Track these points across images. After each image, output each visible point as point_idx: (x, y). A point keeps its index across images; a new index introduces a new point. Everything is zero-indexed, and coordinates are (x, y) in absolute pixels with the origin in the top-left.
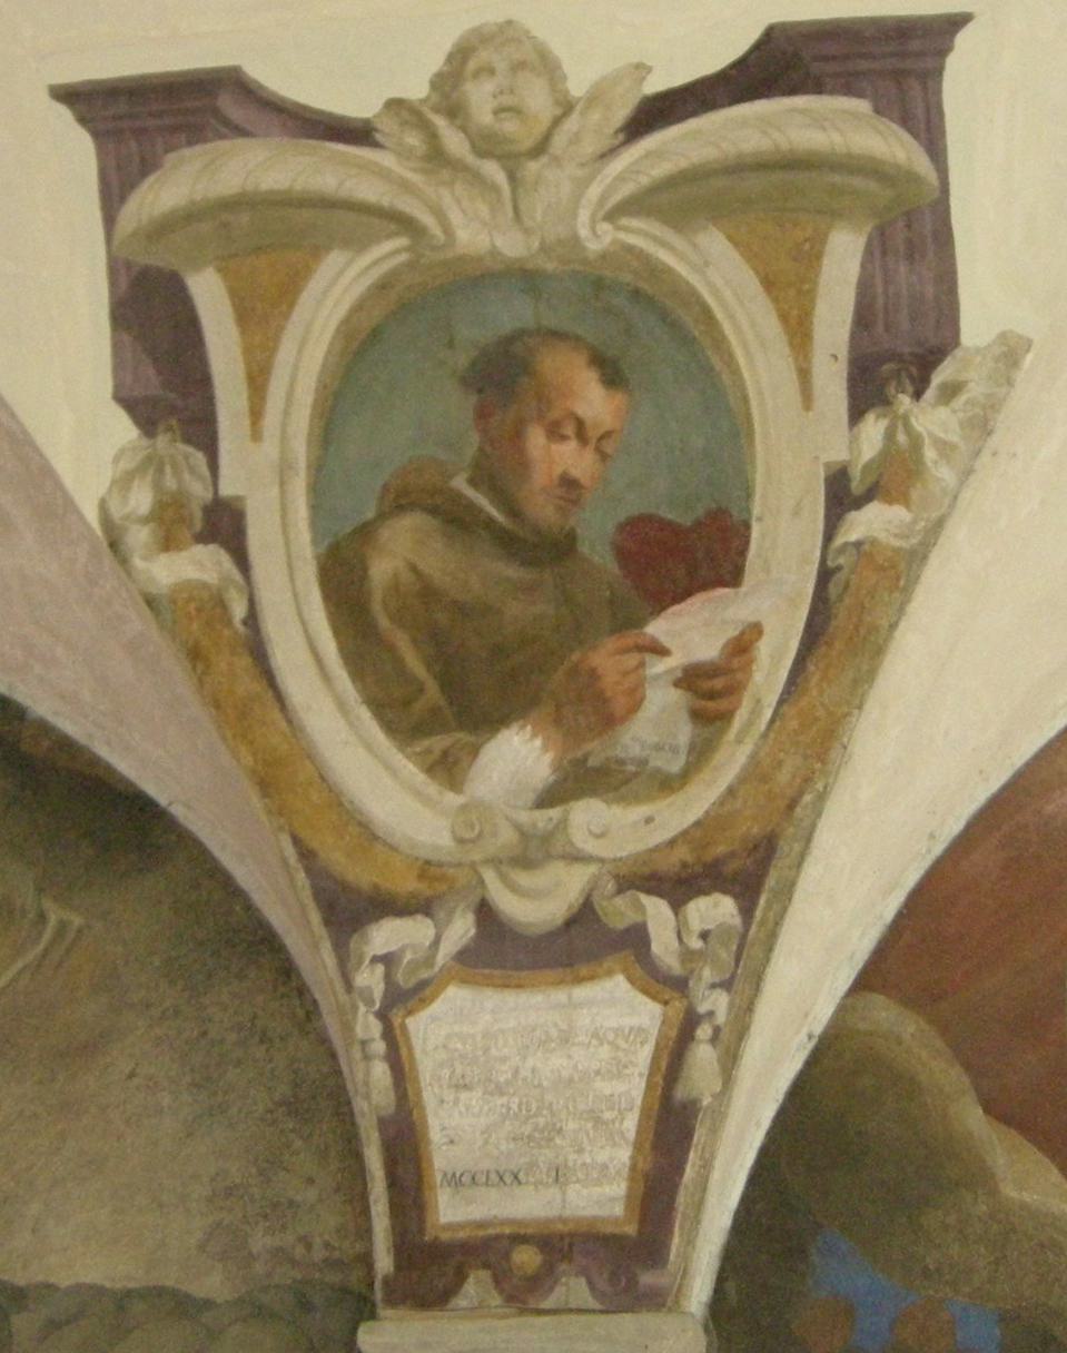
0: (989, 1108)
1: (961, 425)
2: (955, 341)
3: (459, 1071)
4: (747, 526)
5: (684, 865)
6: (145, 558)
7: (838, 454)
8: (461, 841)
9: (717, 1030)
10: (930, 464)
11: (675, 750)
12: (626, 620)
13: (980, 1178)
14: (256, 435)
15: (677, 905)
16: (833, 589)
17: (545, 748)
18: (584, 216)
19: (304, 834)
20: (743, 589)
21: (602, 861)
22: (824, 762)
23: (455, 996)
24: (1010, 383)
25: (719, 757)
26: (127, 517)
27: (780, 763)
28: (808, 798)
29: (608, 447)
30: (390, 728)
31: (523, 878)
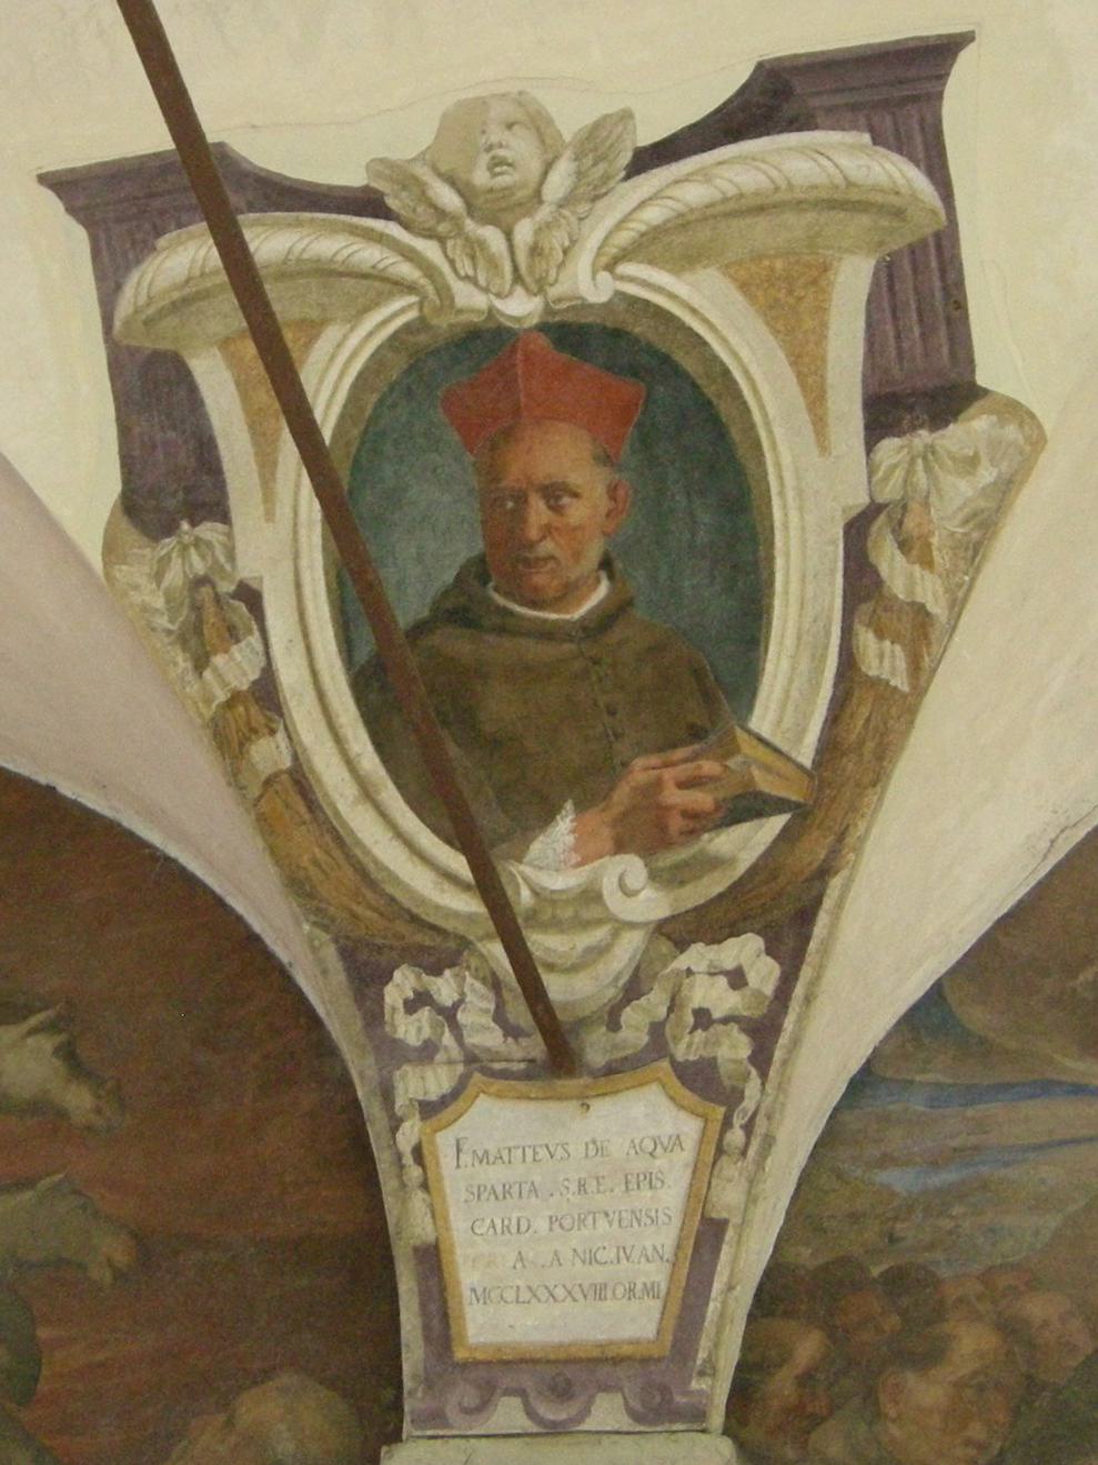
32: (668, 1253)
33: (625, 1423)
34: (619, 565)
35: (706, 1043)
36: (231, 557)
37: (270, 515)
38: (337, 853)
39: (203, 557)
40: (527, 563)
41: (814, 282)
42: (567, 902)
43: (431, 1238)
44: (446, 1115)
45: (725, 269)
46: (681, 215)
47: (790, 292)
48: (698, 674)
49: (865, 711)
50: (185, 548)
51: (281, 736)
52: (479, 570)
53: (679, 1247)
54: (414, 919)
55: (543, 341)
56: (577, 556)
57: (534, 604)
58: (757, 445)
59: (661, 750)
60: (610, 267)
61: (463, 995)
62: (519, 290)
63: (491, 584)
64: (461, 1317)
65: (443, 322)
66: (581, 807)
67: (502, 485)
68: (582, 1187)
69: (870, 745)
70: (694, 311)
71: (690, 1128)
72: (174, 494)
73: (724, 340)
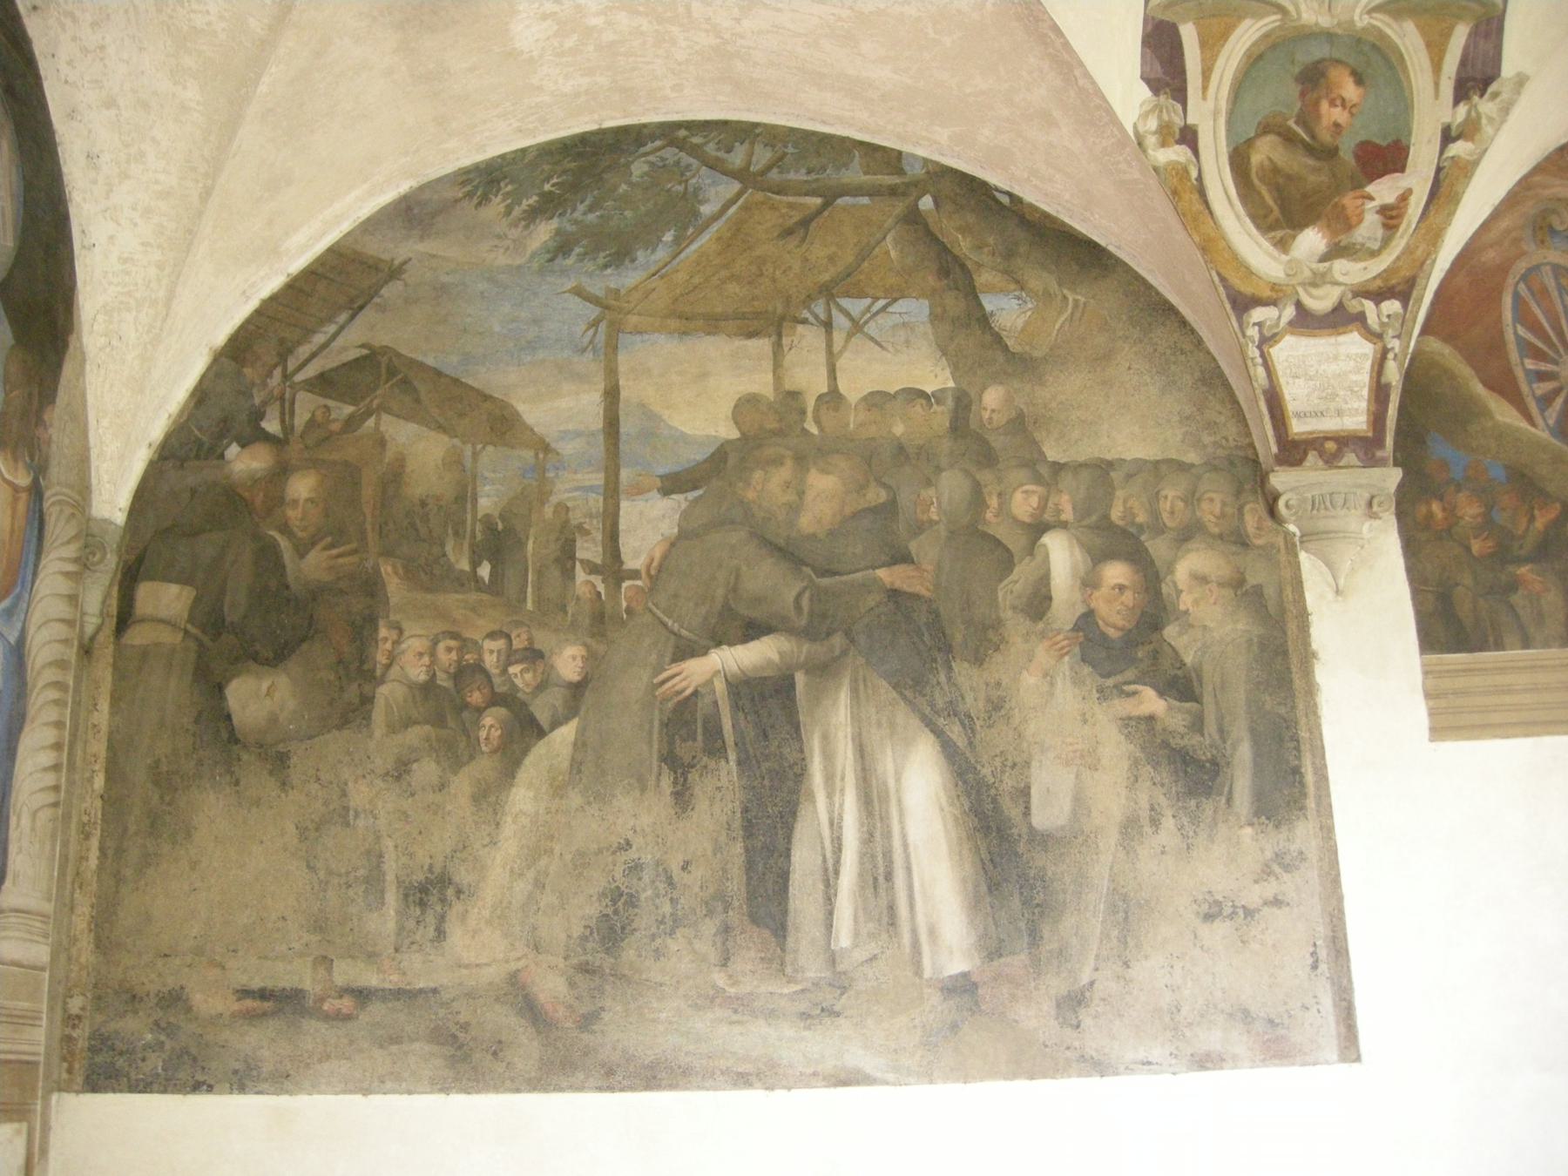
2: (1499, 75)
3: (1294, 370)
4: (1409, 148)
5: (1380, 288)
6: (1154, 150)
7: (1447, 120)
8: (1288, 275)
9: (1396, 355)
11: (1376, 240)
13: (1486, 413)
14: (1204, 98)
15: (1377, 304)
16: (1442, 176)
17: (1323, 237)
18: (1358, 11)
19: (1221, 271)
20: (1406, 174)
21: (1346, 285)
23: (1289, 340)
24: (1519, 93)
25: (1394, 243)
26: (1146, 132)
27: (1417, 247)
28: (1428, 262)
30: (1258, 227)
31: (1314, 291)
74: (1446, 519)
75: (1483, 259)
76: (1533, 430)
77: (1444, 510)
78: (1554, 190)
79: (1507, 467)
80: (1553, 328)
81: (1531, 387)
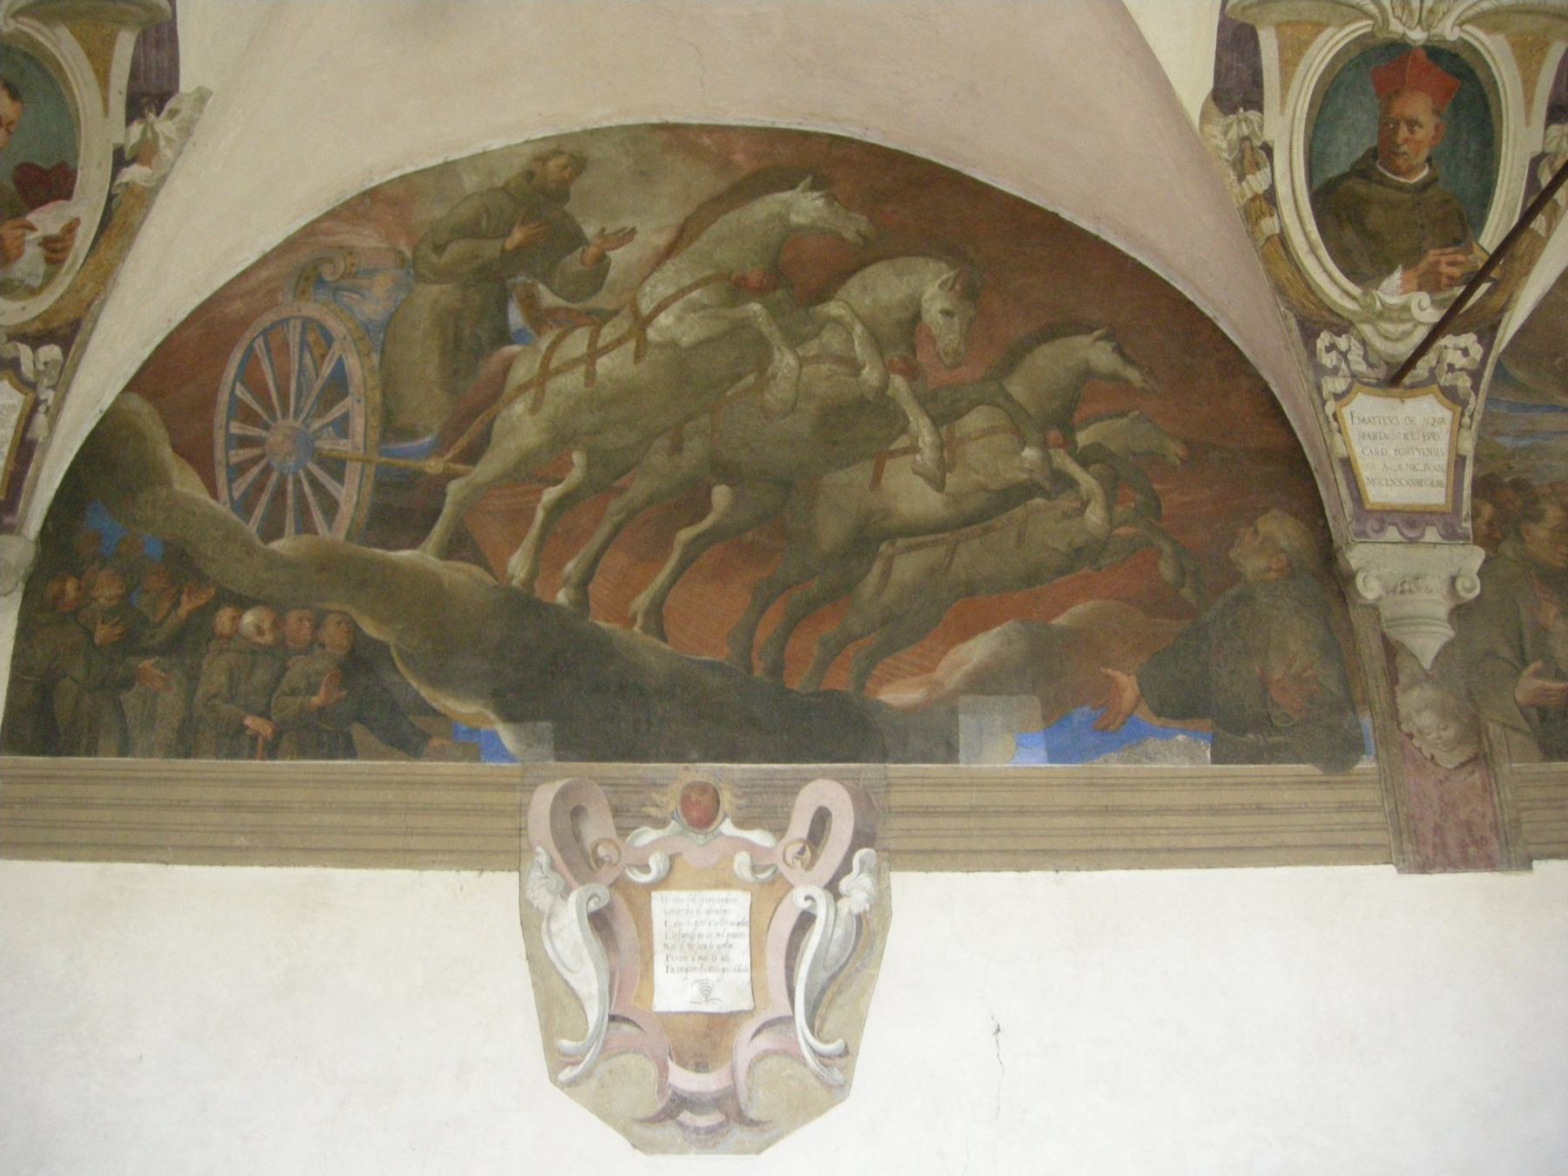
0: (176, 448)
1: (177, 129)
4: (75, 171)
5: (39, 331)
7: (119, 138)
9: (48, 409)
10: (161, 148)
11: (37, 276)
12: (18, 214)
13: (166, 481)
15: (34, 349)
16: (114, 203)
20: (72, 202)
22: (105, 286)
24: (201, 111)
25: (58, 280)
28: (96, 303)
29: (12, 128)
32: (1445, 468)
33: (1439, 539)
34: (1434, 162)
35: (1453, 379)
36: (1261, 127)
37: (1282, 112)
38: (1297, 276)
39: (1248, 126)
40: (1396, 154)
41: (1541, 49)
42: (1397, 310)
43: (1346, 455)
44: (1345, 400)
45: (1508, 36)
46: (1497, 8)
47: (1531, 51)
48: (1461, 216)
49: (1526, 243)
50: (1239, 122)
51: (1275, 217)
52: (1373, 154)
53: (1449, 465)
54: (1330, 310)
55: (1422, 53)
56: (1417, 154)
57: (1396, 174)
58: (1501, 117)
59: (1441, 247)
60: (1461, 25)
61: (1350, 347)
62: (1419, 28)
63: (1378, 162)
64: (1365, 491)
65: (1381, 35)
66: (1406, 268)
67: (1392, 115)
68: (1406, 437)
69: (1526, 257)
70: (1489, 52)
71: (1448, 415)
72: (1238, 94)
73: (1498, 67)
74: (77, 599)
75: (227, 310)
76: (212, 502)
77: (79, 589)
78: (339, 238)
79: (166, 543)
80: (277, 387)
81: (227, 454)
